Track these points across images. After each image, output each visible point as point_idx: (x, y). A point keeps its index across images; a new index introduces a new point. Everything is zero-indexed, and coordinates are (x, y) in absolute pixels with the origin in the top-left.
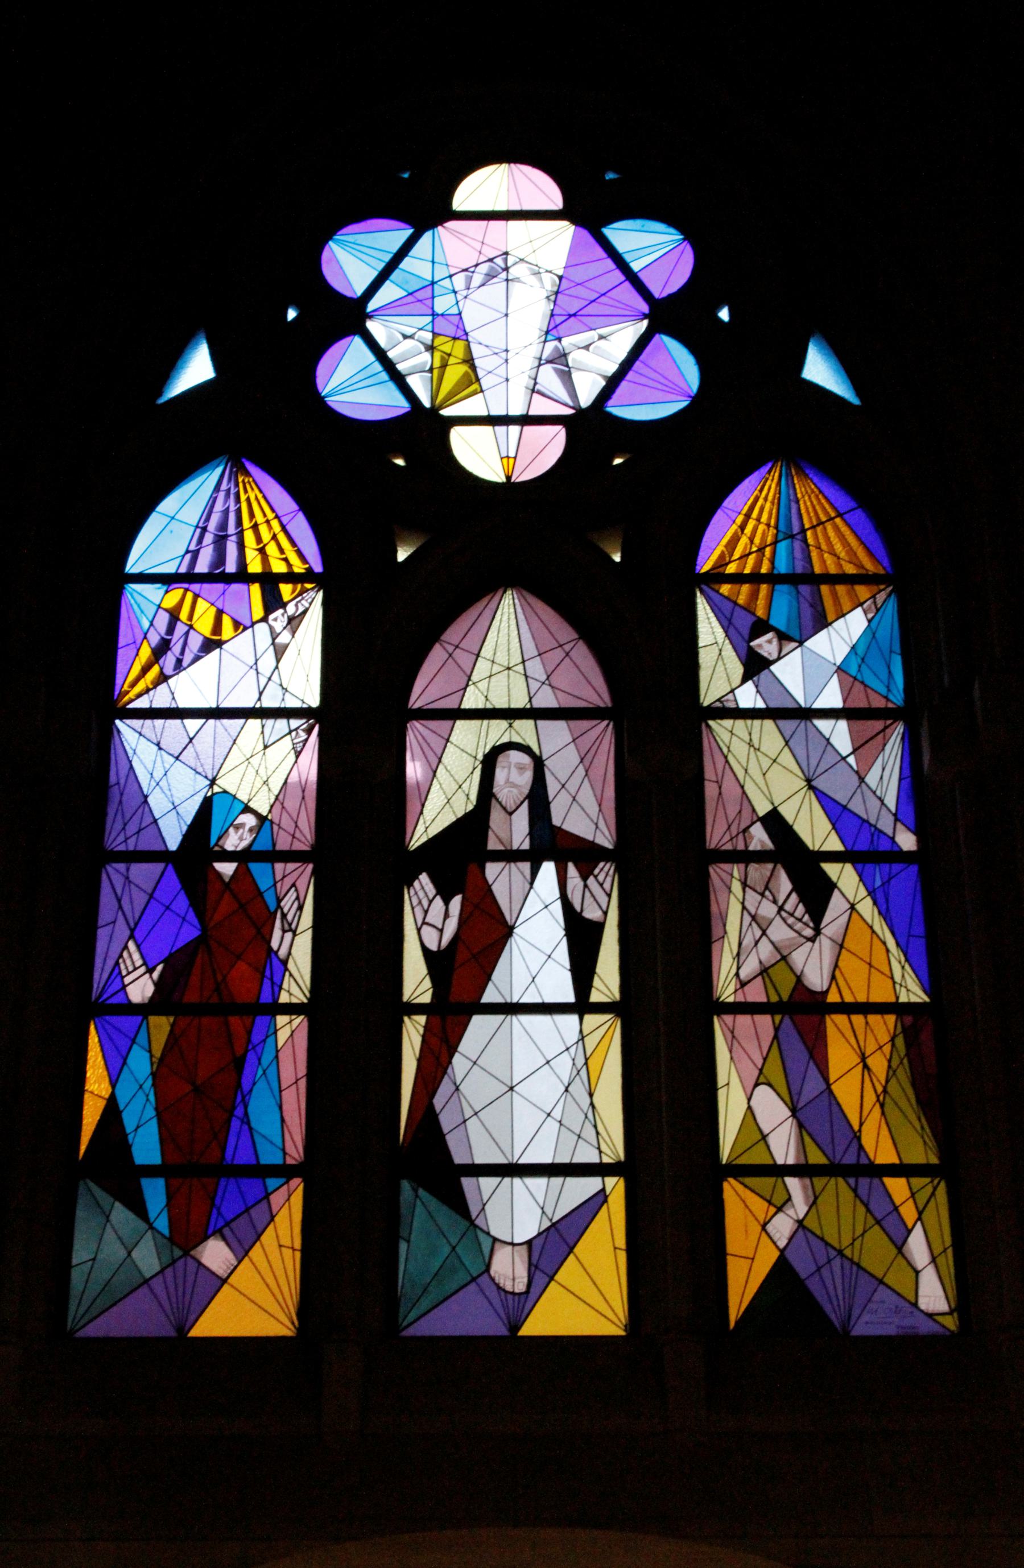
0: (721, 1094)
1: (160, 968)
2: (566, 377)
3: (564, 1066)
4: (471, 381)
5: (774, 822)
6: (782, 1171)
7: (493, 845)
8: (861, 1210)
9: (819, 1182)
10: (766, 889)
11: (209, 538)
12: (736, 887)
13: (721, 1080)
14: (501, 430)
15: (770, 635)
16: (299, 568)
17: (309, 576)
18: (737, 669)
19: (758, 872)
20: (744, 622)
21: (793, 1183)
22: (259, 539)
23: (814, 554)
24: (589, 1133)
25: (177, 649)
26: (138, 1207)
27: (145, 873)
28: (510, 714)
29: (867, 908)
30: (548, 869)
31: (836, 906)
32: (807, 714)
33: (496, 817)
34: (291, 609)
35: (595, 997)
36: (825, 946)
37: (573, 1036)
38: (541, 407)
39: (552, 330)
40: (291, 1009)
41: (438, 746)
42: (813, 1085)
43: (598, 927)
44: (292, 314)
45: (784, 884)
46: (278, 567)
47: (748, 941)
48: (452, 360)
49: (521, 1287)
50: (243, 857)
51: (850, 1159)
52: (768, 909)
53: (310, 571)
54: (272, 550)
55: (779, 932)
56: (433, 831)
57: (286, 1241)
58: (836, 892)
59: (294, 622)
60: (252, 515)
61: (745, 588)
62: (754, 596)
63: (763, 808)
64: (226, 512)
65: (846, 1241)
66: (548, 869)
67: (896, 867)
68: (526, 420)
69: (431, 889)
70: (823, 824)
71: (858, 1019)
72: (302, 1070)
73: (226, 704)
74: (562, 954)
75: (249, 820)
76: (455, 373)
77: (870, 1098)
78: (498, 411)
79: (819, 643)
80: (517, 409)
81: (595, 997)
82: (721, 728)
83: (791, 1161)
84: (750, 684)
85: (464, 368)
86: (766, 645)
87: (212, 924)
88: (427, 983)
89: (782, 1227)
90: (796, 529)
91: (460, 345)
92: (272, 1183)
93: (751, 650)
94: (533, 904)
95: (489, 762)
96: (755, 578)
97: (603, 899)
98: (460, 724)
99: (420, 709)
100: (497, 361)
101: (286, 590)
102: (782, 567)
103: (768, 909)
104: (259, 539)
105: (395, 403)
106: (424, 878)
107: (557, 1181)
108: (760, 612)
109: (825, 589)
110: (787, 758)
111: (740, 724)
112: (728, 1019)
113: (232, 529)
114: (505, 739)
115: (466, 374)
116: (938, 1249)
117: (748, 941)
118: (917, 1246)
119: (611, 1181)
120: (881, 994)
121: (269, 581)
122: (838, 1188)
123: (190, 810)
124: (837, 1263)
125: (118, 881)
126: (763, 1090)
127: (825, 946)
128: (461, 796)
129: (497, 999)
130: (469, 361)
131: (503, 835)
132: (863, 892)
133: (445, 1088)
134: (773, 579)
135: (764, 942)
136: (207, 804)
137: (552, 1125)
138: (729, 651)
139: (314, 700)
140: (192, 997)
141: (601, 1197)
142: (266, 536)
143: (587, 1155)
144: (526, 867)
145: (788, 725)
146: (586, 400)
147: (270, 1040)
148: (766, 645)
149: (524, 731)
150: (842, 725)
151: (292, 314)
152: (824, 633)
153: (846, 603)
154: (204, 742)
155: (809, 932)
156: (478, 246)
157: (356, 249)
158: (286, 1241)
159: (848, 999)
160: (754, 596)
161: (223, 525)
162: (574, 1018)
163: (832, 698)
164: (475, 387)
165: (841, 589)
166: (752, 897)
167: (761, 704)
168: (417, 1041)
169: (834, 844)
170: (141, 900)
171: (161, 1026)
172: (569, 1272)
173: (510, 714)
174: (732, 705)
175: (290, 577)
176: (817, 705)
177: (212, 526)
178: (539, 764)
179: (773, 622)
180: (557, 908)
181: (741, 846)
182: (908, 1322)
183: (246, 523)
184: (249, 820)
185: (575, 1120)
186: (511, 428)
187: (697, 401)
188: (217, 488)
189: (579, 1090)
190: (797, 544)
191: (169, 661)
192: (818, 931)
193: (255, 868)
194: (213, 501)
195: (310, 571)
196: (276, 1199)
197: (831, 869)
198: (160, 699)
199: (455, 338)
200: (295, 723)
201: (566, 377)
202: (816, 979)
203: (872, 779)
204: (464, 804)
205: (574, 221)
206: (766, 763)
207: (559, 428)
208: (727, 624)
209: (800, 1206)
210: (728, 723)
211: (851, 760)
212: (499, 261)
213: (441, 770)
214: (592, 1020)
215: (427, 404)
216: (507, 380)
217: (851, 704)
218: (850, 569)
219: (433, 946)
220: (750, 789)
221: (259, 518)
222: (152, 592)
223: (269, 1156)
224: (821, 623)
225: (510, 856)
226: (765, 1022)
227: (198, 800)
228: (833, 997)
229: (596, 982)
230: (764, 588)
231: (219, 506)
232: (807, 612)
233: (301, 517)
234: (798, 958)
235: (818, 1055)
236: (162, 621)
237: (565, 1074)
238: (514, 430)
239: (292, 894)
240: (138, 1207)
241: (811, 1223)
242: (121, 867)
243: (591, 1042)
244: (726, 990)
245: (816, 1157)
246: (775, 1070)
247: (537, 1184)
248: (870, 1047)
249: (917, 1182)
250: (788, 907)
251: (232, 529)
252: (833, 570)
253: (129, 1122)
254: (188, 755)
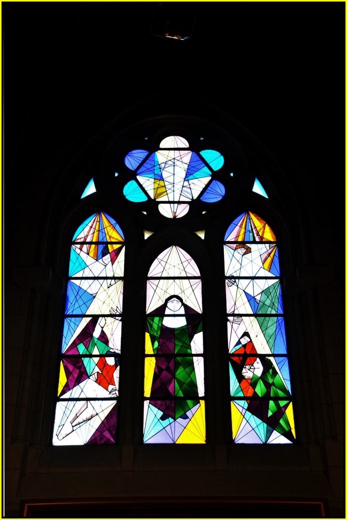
14: (172, 205)
38: (183, 199)
44: (116, 175)
68: (179, 203)
78: (171, 200)
99: (151, 277)
100: (171, 186)
105: (145, 199)
139: (122, 275)
146: (195, 197)
151: (116, 175)
156: (166, 157)
164: (165, 193)
186: (175, 204)
187: (224, 197)
199: (160, 180)
205: (192, 151)
207: (187, 205)
215: (153, 198)
216: (174, 191)
233: (117, 225)
238: (176, 205)
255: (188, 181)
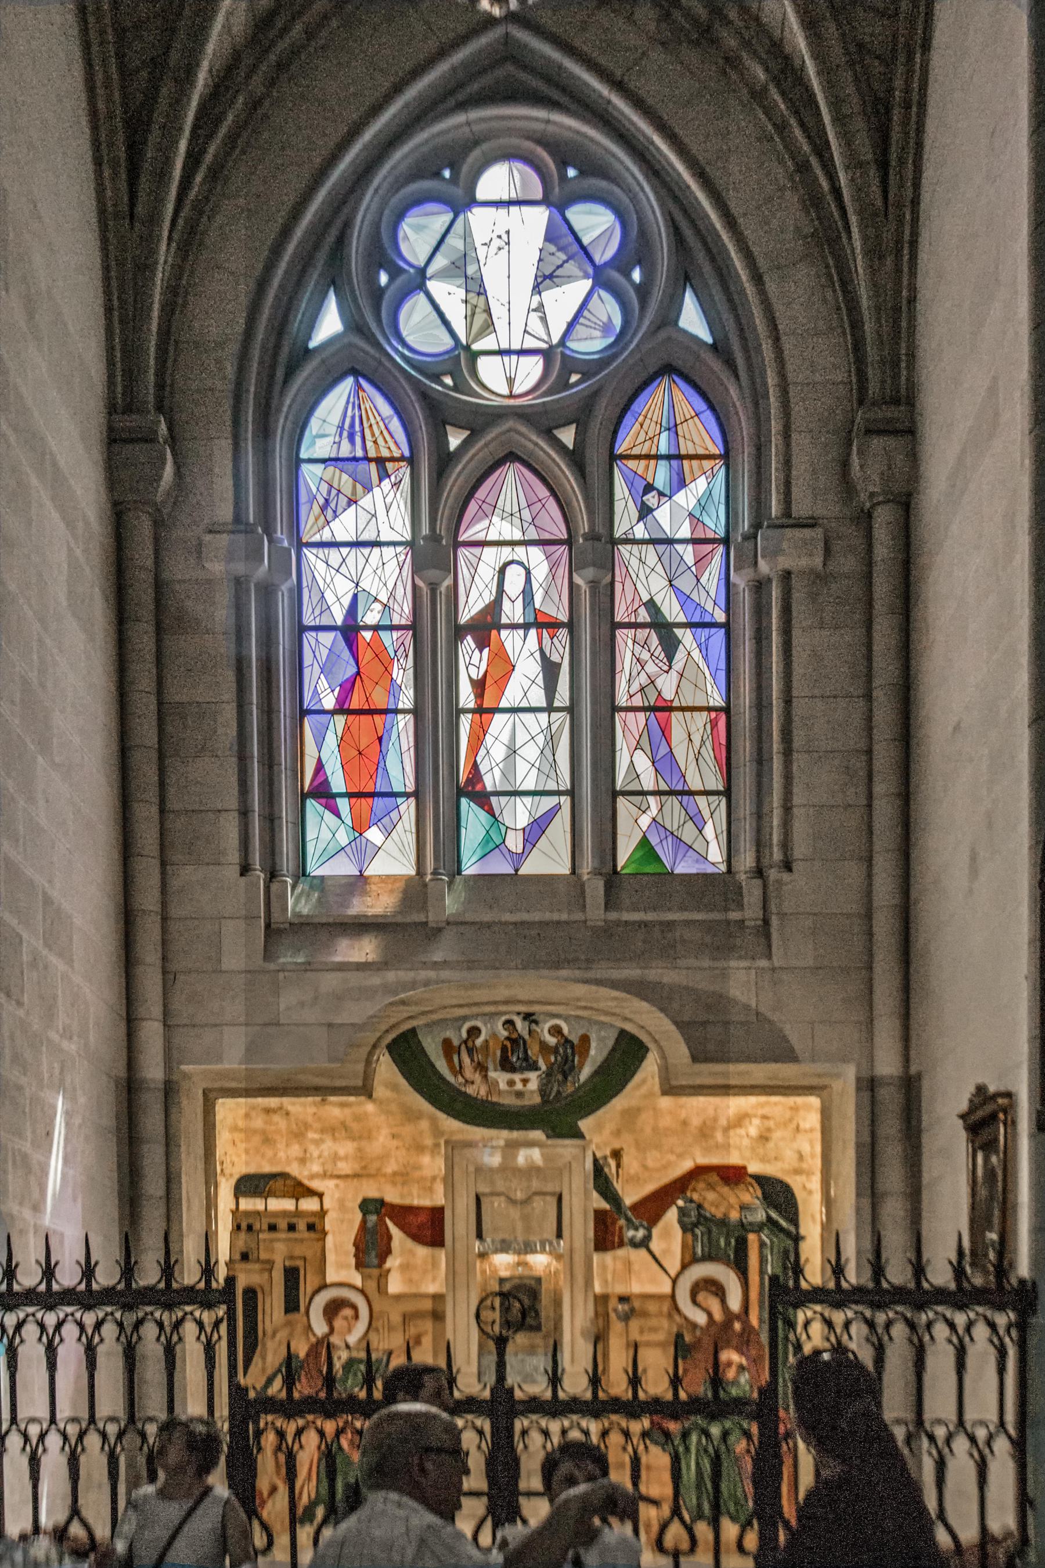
0: (618, 754)
1: (338, 689)
2: (544, 320)
3: (541, 740)
4: (489, 326)
5: (651, 605)
6: (643, 793)
7: (504, 620)
8: (683, 812)
9: (664, 798)
10: (645, 644)
11: (345, 434)
12: (630, 642)
13: (618, 747)
14: (506, 359)
15: (654, 493)
16: (397, 454)
17: (402, 458)
18: (634, 514)
19: (641, 634)
20: (640, 485)
21: (651, 800)
22: (373, 435)
23: (681, 440)
24: (553, 775)
25: (333, 505)
26: (337, 813)
27: (327, 638)
28: (512, 543)
29: (696, 654)
30: (533, 632)
31: (680, 655)
32: (670, 542)
33: (506, 605)
34: (393, 478)
35: (556, 704)
36: (674, 675)
37: (545, 725)
38: (531, 343)
39: (537, 289)
40: (404, 711)
41: (474, 560)
42: (663, 750)
43: (559, 666)
45: (654, 641)
46: (385, 453)
47: (634, 673)
48: (478, 310)
49: (520, 851)
50: (376, 628)
51: (679, 787)
52: (645, 656)
53: (403, 455)
54: (380, 441)
55: (651, 668)
56: (473, 612)
57: (407, 828)
58: (681, 647)
59: (396, 485)
60: (368, 419)
61: (643, 463)
62: (647, 467)
63: (645, 598)
64: (353, 418)
65: (675, 827)
66: (533, 632)
67: (713, 630)
69: (473, 646)
70: (676, 606)
71: (688, 714)
72: (412, 744)
73: (362, 538)
74: (540, 680)
75: (377, 606)
76: (480, 319)
77: (691, 756)
79: (680, 497)
80: (516, 346)
81: (556, 704)
82: (624, 550)
83: (651, 788)
84: (641, 524)
85: (485, 316)
86: (651, 499)
87: (365, 662)
88: (472, 697)
89: (645, 821)
90: (672, 424)
91: (482, 298)
92: (400, 800)
93: (643, 503)
94: (525, 653)
95: (502, 571)
96: (648, 457)
97: (561, 650)
98: (486, 549)
101: (389, 466)
102: (663, 449)
103: (645, 656)
104: (373, 435)
106: (469, 638)
107: (537, 798)
108: (650, 480)
109: (686, 463)
110: (659, 568)
111: (635, 547)
112: (623, 714)
113: (357, 428)
114: (510, 558)
115: (486, 321)
116: (719, 831)
117: (634, 673)
118: (709, 831)
119: (563, 798)
120: (701, 702)
121: (380, 461)
122: (674, 802)
123: (346, 601)
124: (670, 839)
125: (313, 642)
126: (639, 752)
127: (674, 675)
128: (487, 592)
129: (508, 705)
130: (488, 311)
131: (510, 614)
132: (695, 645)
133: (482, 752)
134: (657, 457)
135: (643, 674)
136: (355, 597)
137: (535, 771)
138: (631, 503)
140: (355, 705)
141: (558, 807)
142: (377, 433)
143: (552, 786)
144: (521, 632)
145: (661, 548)
147: (395, 728)
148: (651, 499)
149: (520, 552)
150: (690, 547)
152: (683, 492)
153: (697, 473)
154: (351, 560)
155: (666, 668)
157: (418, 228)
158: (407, 828)
159: (684, 704)
160: (647, 467)
161: (352, 425)
162: (546, 715)
163: (685, 532)
165: (695, 463)
166: (638, 648)
167: (647, 536)
168: (468, 727)
169: (682, 618)
170: (325, 653)
171: (340, 720)
172: (543, 842)
173: (512, 543)
174: (631, 537)
175: (393, 459)
176: (677, 536)
177: (347, 426)
178: (528, 573)
179: (656, 485)
180: (537, 655)
181: (633, 620)
182: (702, 866)
183: (366, 425)
184: (377, 606)
185: (546, 768)
188: (348, 402)
189: (548, 752)
190: (673, 435)
191: (329, 513)
192: (670, 667)
193: (382, 633)
194: (346, 409)
195: (403, 455)
196: (402, 808)
197: (679, 632)
198: (326, 536)
200: (399, 549)
201: (544, 320)
202: (668, 694)
203: (703, 580)
204: (488, 597)
206: (648, 571)
208: (631, 486)
209: (654, 811)
210: (629, 547)
211: (693, 569)
212: (505, 237)
213: (476, 577)
214: (555, 716)
215: (464, 342)
217: (696, 536)
218: (701, 451)
219: (474, 677)
220: (639, 586)
221: (373, 421)
222: (318, 469)
223: (398, 788)
224: (682, 484)
225: (513, 626)
226: (641, 716)
227: (350, 596)
228: (676, 704)
229: (557, 695)
230: (653, 462)
231: (349, 413)
232: (675, 477)
234: (659, 683)
235: (666, 732)
236: (324, 488)
237: (541, 743)
238: (514, 358)
239: (402, 649)
240: (337, 813)
241: (659, 819)
242: (314, 634)
243: (554, 728)
244: (622, 700)
245: (663, 787)
246: (645, 743)
247: (528, 800)
248: (693, 729)
249: (711, 798)
250: (656, 654)
251: (357, 428)
252: (692, 452)
253: (328, 769)
254: (343, 569)
255: (540, 293)
